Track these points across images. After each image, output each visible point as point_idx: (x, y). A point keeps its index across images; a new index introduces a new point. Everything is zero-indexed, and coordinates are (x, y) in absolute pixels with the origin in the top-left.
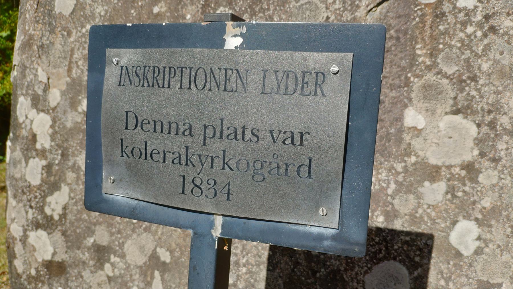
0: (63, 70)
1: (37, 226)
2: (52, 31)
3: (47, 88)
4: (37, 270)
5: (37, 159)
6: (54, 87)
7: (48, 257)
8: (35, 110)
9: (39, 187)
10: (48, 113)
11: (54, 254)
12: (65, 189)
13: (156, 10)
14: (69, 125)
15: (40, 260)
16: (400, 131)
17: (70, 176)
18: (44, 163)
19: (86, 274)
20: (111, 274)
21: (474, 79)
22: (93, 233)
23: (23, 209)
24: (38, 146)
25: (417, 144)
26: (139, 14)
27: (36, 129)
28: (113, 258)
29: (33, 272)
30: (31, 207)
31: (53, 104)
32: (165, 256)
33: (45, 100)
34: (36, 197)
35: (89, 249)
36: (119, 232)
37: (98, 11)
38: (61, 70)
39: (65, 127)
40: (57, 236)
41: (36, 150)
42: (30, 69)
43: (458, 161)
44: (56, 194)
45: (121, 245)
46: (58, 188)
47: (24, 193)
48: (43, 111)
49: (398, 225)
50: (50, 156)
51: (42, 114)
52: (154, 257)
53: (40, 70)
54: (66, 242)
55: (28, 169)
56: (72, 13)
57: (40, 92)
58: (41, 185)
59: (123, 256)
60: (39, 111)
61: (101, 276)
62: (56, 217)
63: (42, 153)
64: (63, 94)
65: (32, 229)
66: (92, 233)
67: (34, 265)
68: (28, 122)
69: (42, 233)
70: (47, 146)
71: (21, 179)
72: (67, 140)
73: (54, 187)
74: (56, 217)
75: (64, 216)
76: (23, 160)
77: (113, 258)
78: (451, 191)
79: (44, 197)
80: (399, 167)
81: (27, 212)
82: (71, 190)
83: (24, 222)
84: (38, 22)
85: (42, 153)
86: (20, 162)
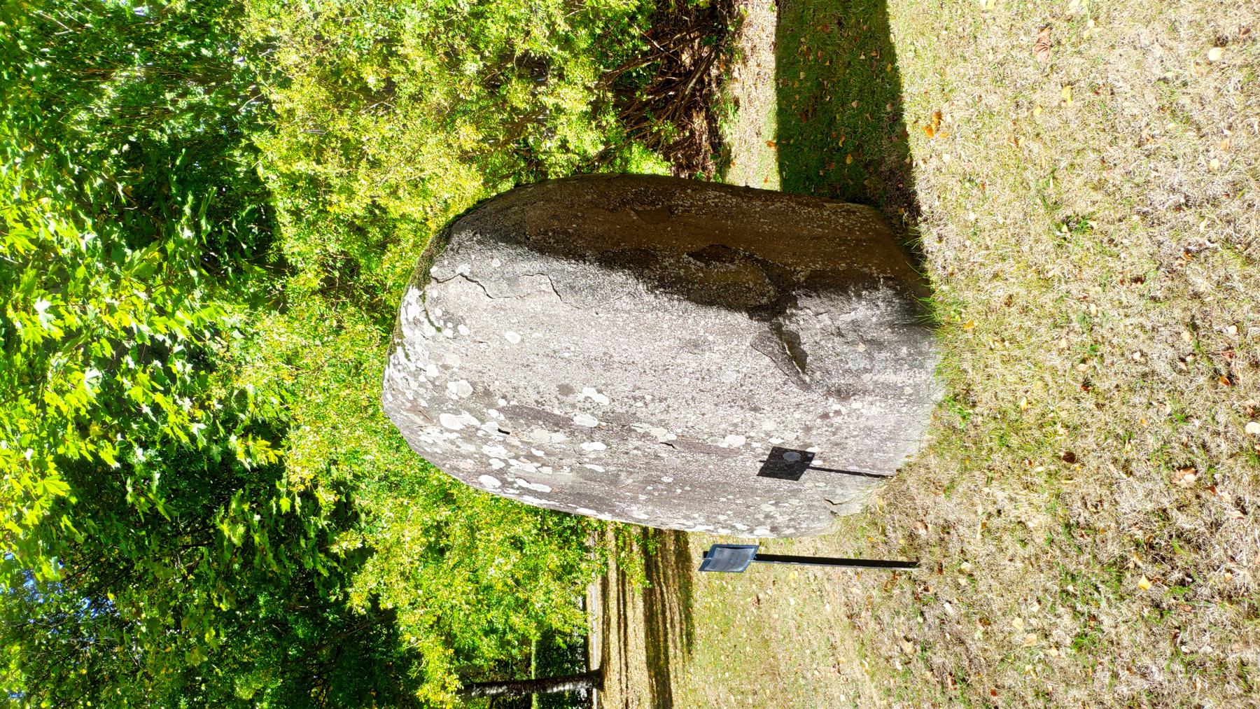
49: (768, 453)
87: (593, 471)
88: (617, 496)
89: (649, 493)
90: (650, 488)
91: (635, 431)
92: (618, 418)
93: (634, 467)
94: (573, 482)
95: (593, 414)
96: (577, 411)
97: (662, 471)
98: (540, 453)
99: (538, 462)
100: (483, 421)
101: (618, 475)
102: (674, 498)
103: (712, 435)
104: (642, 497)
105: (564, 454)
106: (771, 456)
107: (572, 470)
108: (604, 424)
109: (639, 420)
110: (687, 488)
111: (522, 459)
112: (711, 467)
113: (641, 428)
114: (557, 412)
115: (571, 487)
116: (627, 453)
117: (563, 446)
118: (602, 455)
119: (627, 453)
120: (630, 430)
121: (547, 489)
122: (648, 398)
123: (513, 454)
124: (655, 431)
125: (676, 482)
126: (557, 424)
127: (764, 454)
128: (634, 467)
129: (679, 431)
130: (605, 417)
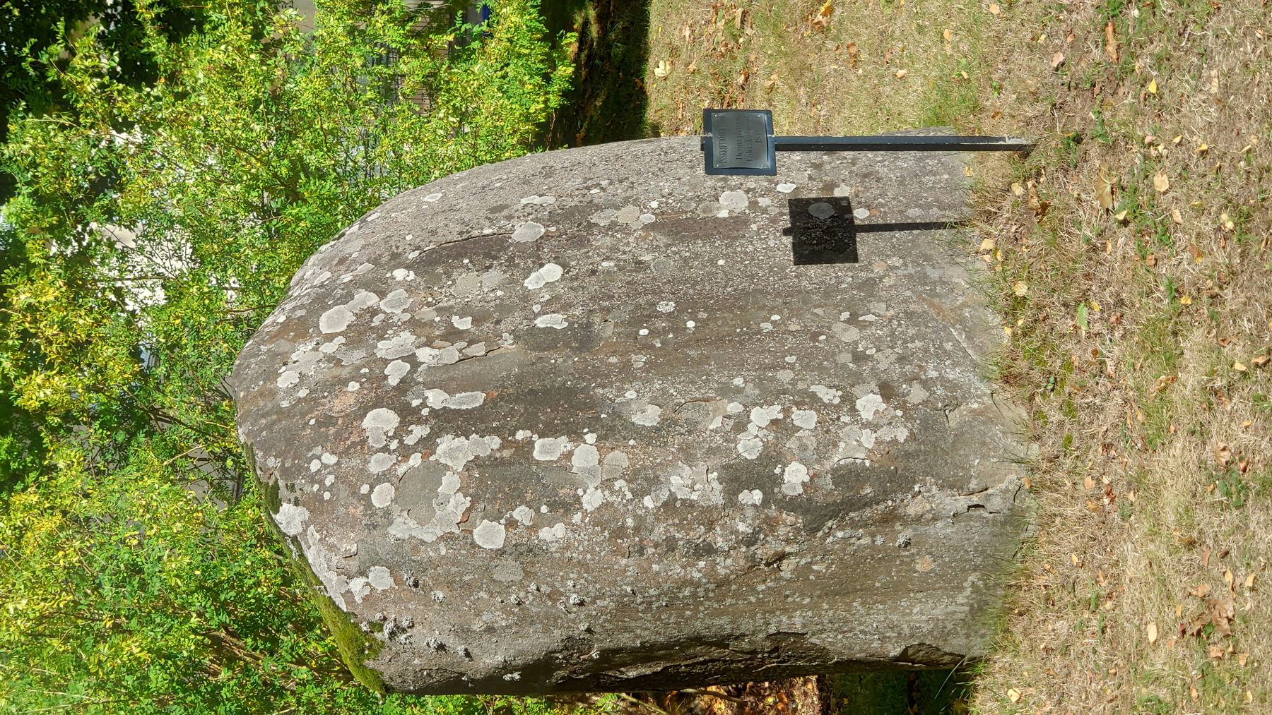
0: (710, 407)
1: (853, 411)
2: (676, 423)
3: (729, 417)
4: (896, 408)
5: (793, 416)
6: (726, 411)
7: (879, 398)
8: (749, 426)
9: (818, 411)
10: (750, 412)
11: (874, 393)
12: (813, 388)
13: (659, 345)
14: (757, 392)
15: (885, 406)
16: (731, 218)
17: (800, 386)
18: (794, 409)
19: (882, 367)
20: (874, 350)
21: (698, 197)
22: (843, 364)
23: (844, 430)
24: (781, 416)
25: (738, 211)
26: (661, 357)
27: (765, 424)
28: (860, 348)
29: (900, 413)
30: (838, 418)
31: (741, 408)
32: (845, 315)
33: (738, 415)
34: (828, 414)
35: (859, 366)
36: (837, 347)
37: (658, 386)
38: (711, 408)
39: (759, 395)
40: (857, 390)
41: (784, 418)
42: (711, 441)
43: (745, 196)
44: (820, 395)
45: (848, 344)
46: (814, 394)
47: (827, 431)
48: (748, 417)
49: (787, 211)
50: (788, 404)
51: (752, 417)
52: (848, 321)
53: (711, 427)
54: (859, 384)
55: (805, 426)
56: (659, 406)
57: (732, 423)
58: (815, 410)
59: (856, 343)
60: (749, 422)
61: (879, 356)
62: (840, 393)
63: (787, 411)
64: (731, 401)
65: (859, 415)
66: (844, 366)
67: (893, 412)
68: (761, 435)
69: (859, 404)
70: (779, 408)
71: (815, 436)
72: (771, 392)
73: (813, 396)
74: (840, 393)
75: (838, 388)
76: (797, 435)
77: (860, 348)
78: (762, 196)
79: (826, 406)
80: (752, 215)
81: (846, 424)
82: (813, 384)
83: (855, 428)
84: (666, 443)
85: (787, 411)
86: (800, 439)
87: (549, 331)
88: (597, 373)
89: (647, 347)
90: (644, 332)
91: (596, 225)
92: (568, 214)
93: (611, 297)
94: (521, 365)
95: (536, 220)
96: (514, 221)
97: (653, 292)
98: (463, 324)
99: (462, 339)
100: (382, 295)
101: (589, 325)
102: (687, 345)
103: (700, 200)
104: (639, 360)
105: (504, 309)
106: (792, 214)
107: (517, 338)
108: (553, 229)
109: (599, 208)
110: (703, 315)
111: (438, 342)
112: (721, 262)
113: (601, 219)
114: (487, 231)
115: (520, 379)
116: (594, 272)
117: (499, 293)
118: (560, 290)
119: (594, 272)
120: (591, 226)
121: (477, 399)
122: (604, 183)
123: (424, 339)
124: (626, 215)
125: (687, 307)
126: (488, 255)
127: (782, 214)
128: (611, 297)
129: (654, 204)
130: (553, 218)
